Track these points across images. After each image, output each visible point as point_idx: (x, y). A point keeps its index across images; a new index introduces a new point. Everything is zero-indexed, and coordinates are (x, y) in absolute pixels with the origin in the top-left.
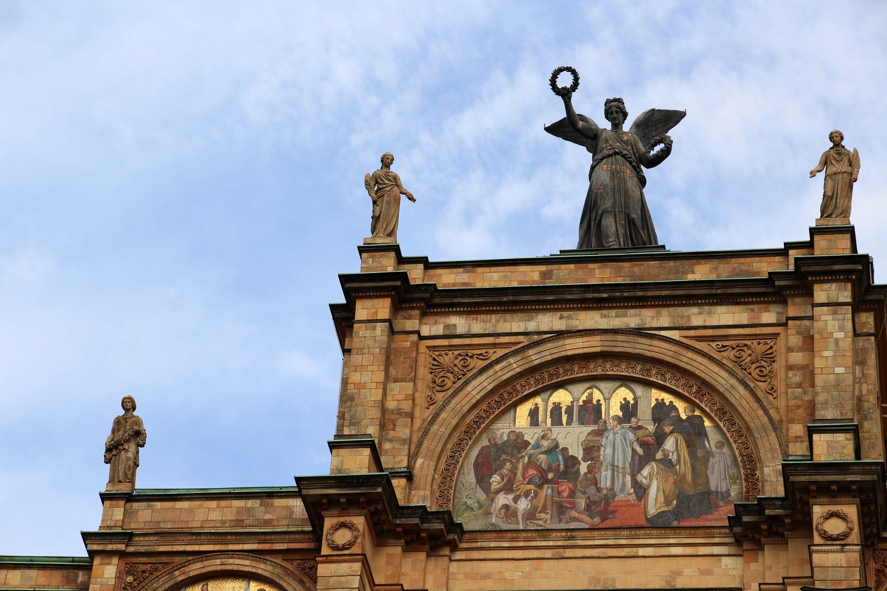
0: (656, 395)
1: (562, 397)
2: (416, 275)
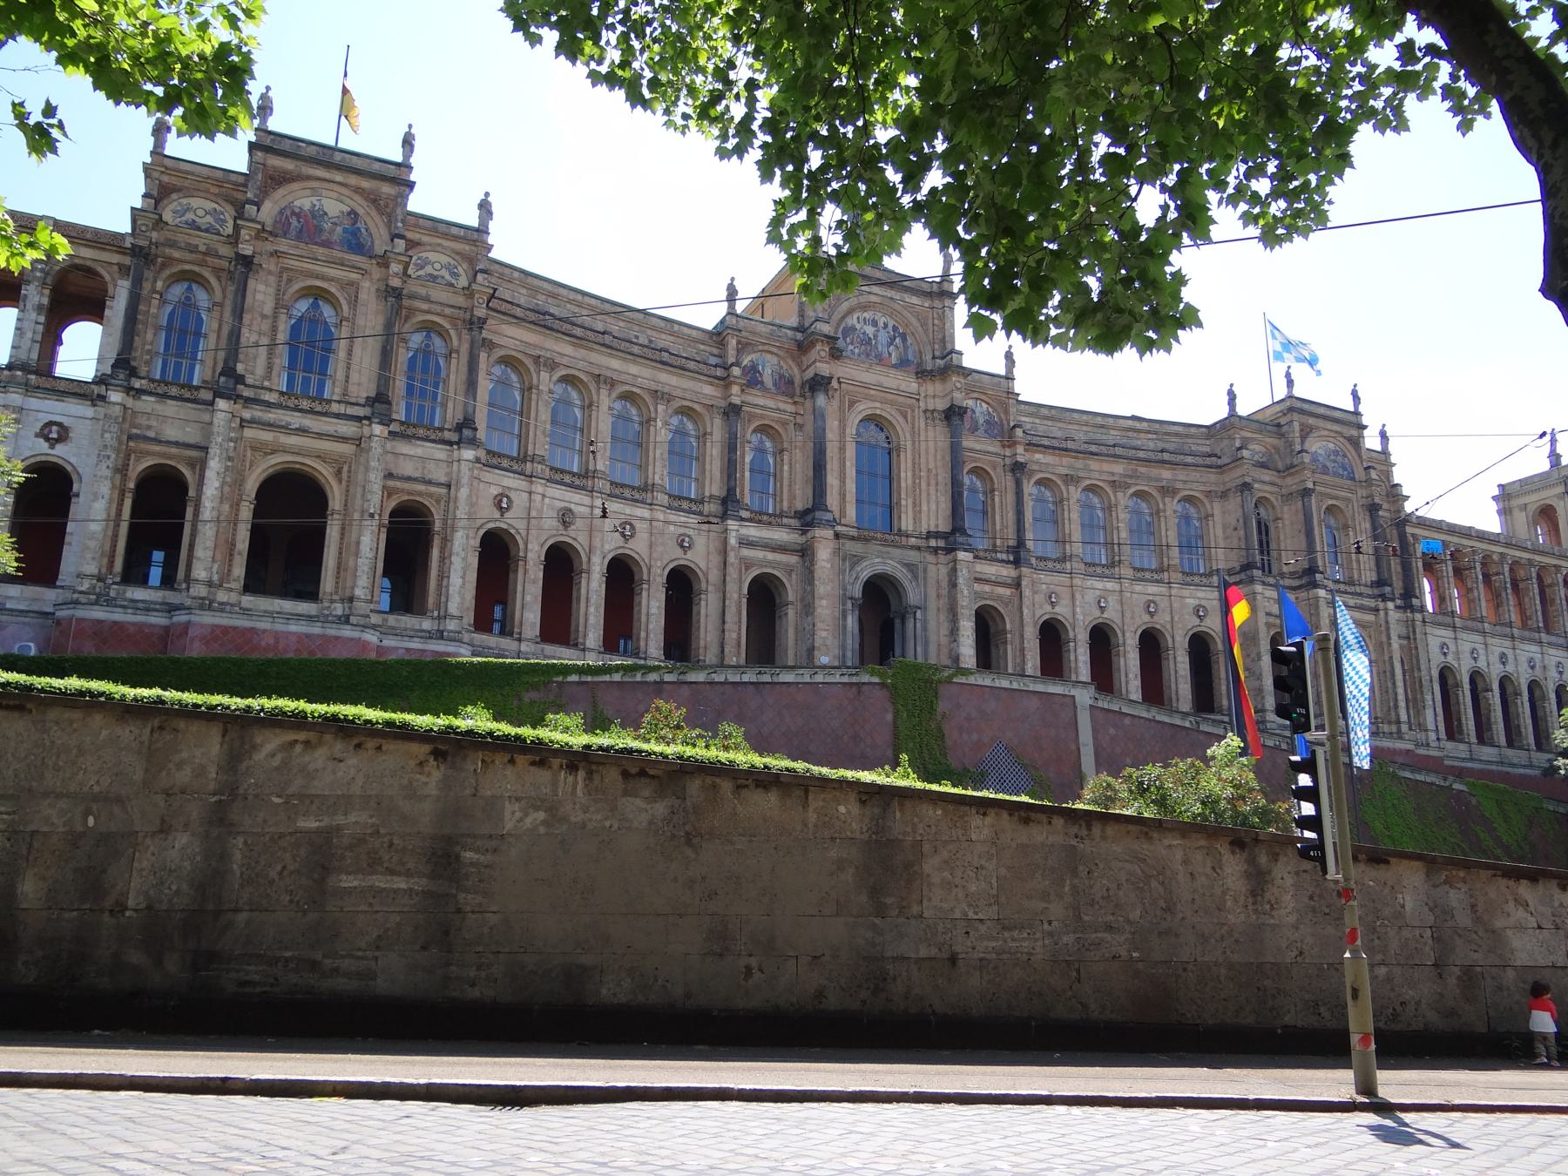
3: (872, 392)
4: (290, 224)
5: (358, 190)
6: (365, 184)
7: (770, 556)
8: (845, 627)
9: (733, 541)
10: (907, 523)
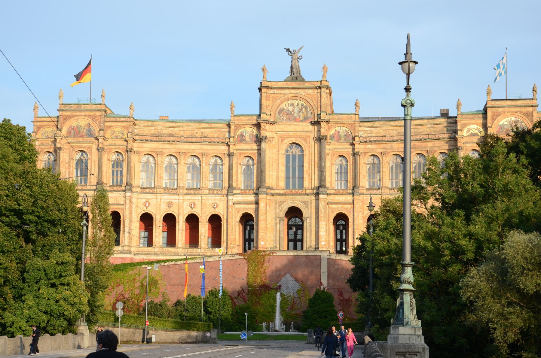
0: (301, 102)
1: (289, 102)
2: (269, 84)
3: (291, 134)
4: (71, 132)
5: (90, 116)
6: (91, 113)
7: (247, 206)
8: (276, 229)
9: (230, 203)
10: (306, 184)
